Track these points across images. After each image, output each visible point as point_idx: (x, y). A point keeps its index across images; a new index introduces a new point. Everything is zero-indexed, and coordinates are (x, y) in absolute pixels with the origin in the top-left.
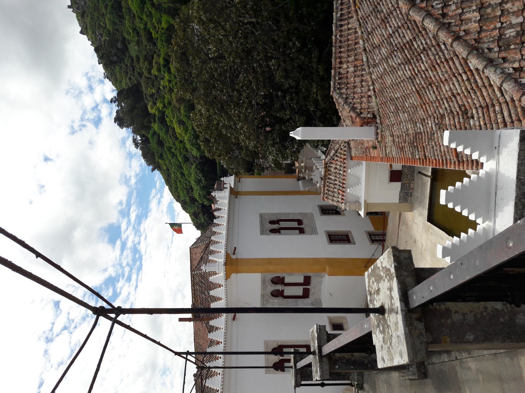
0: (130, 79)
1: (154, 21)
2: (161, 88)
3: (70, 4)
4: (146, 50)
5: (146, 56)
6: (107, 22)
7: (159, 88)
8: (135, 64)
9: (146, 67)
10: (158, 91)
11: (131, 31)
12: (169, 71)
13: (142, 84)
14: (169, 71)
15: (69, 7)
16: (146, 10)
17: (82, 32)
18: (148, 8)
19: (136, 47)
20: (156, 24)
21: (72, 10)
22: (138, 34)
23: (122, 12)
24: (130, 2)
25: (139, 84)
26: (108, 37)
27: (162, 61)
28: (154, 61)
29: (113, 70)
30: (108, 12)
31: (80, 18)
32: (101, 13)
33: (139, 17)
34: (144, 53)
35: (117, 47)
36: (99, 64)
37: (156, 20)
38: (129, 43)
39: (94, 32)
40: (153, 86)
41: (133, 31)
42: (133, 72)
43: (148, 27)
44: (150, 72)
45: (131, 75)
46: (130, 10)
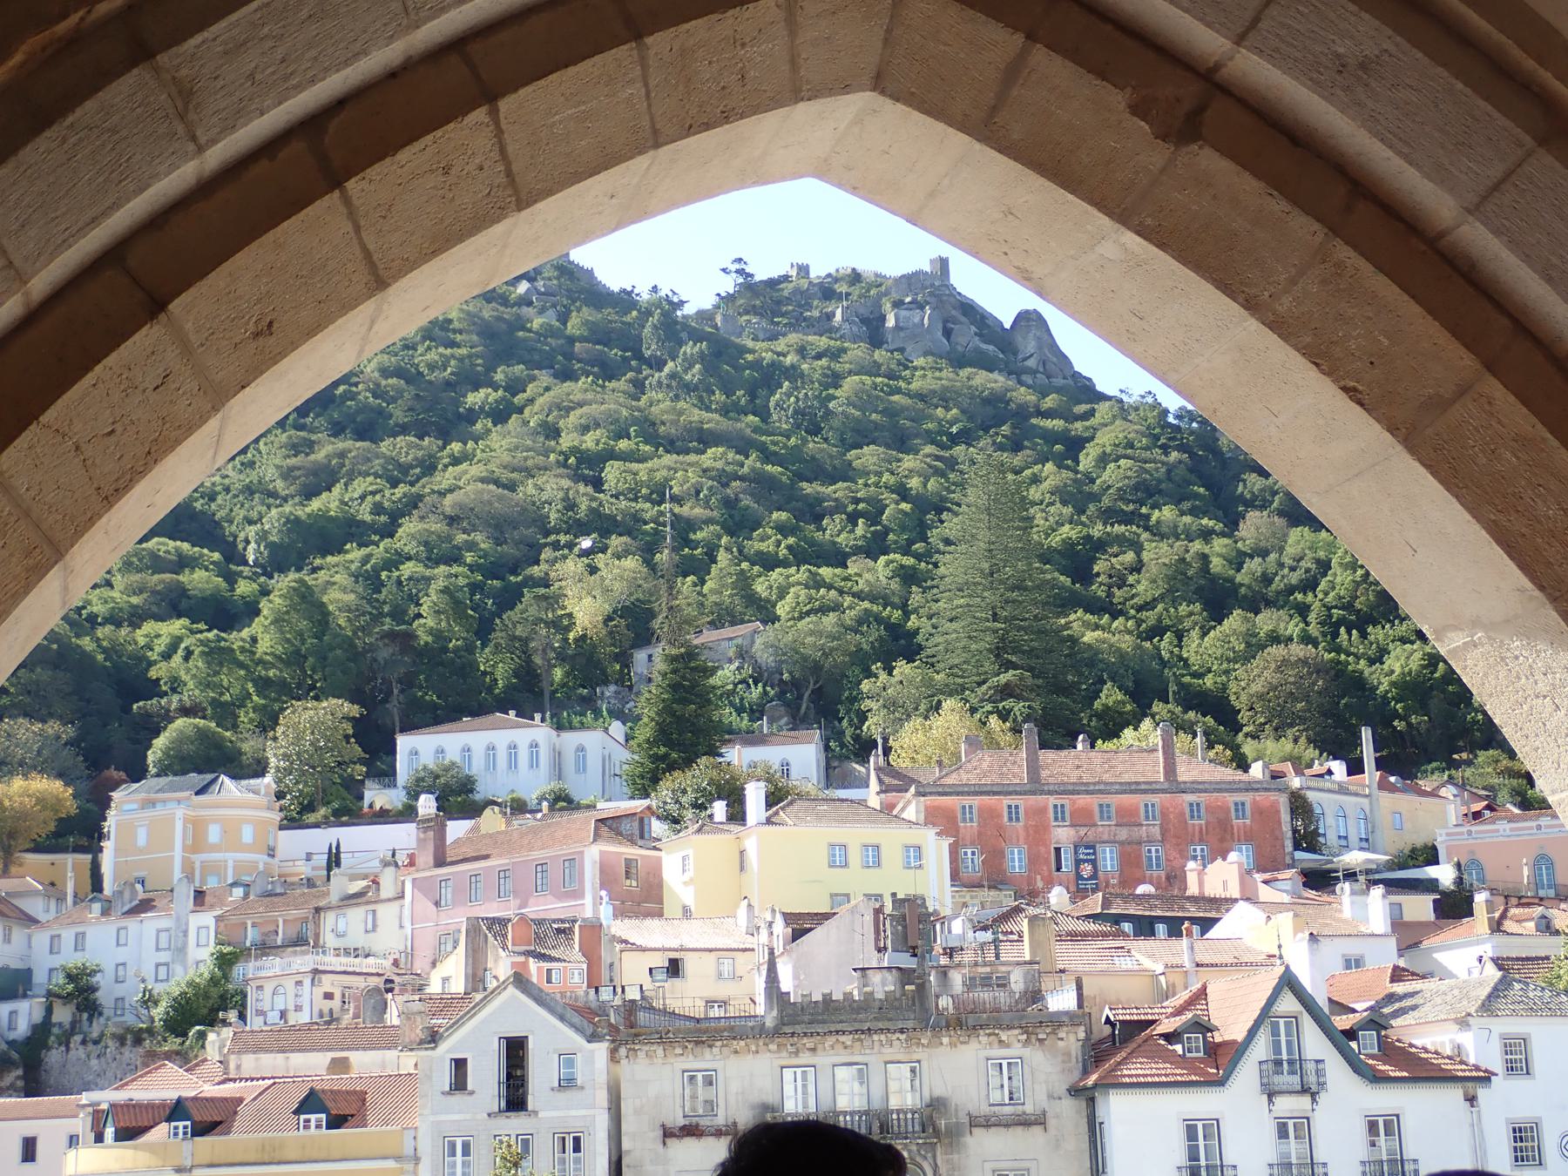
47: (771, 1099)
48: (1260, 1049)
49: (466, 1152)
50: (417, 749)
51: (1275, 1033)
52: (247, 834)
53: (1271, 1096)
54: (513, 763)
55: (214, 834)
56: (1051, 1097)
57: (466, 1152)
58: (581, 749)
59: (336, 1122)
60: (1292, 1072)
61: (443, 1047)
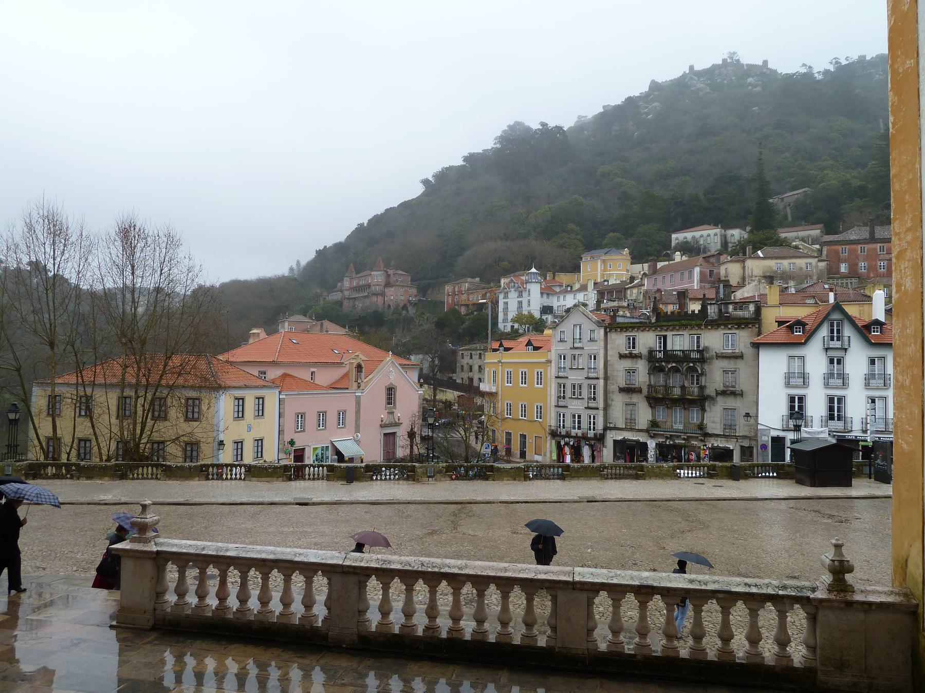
3: (696, 68)
17: (653, 82)
36: (604, 107)
47: (652, 346)
48: (824, 331)
50: (677, 237)
51: (832, 325)
53: (827, 349)
56: (745, 346)
59: (536, 349)
60: (838, 339)
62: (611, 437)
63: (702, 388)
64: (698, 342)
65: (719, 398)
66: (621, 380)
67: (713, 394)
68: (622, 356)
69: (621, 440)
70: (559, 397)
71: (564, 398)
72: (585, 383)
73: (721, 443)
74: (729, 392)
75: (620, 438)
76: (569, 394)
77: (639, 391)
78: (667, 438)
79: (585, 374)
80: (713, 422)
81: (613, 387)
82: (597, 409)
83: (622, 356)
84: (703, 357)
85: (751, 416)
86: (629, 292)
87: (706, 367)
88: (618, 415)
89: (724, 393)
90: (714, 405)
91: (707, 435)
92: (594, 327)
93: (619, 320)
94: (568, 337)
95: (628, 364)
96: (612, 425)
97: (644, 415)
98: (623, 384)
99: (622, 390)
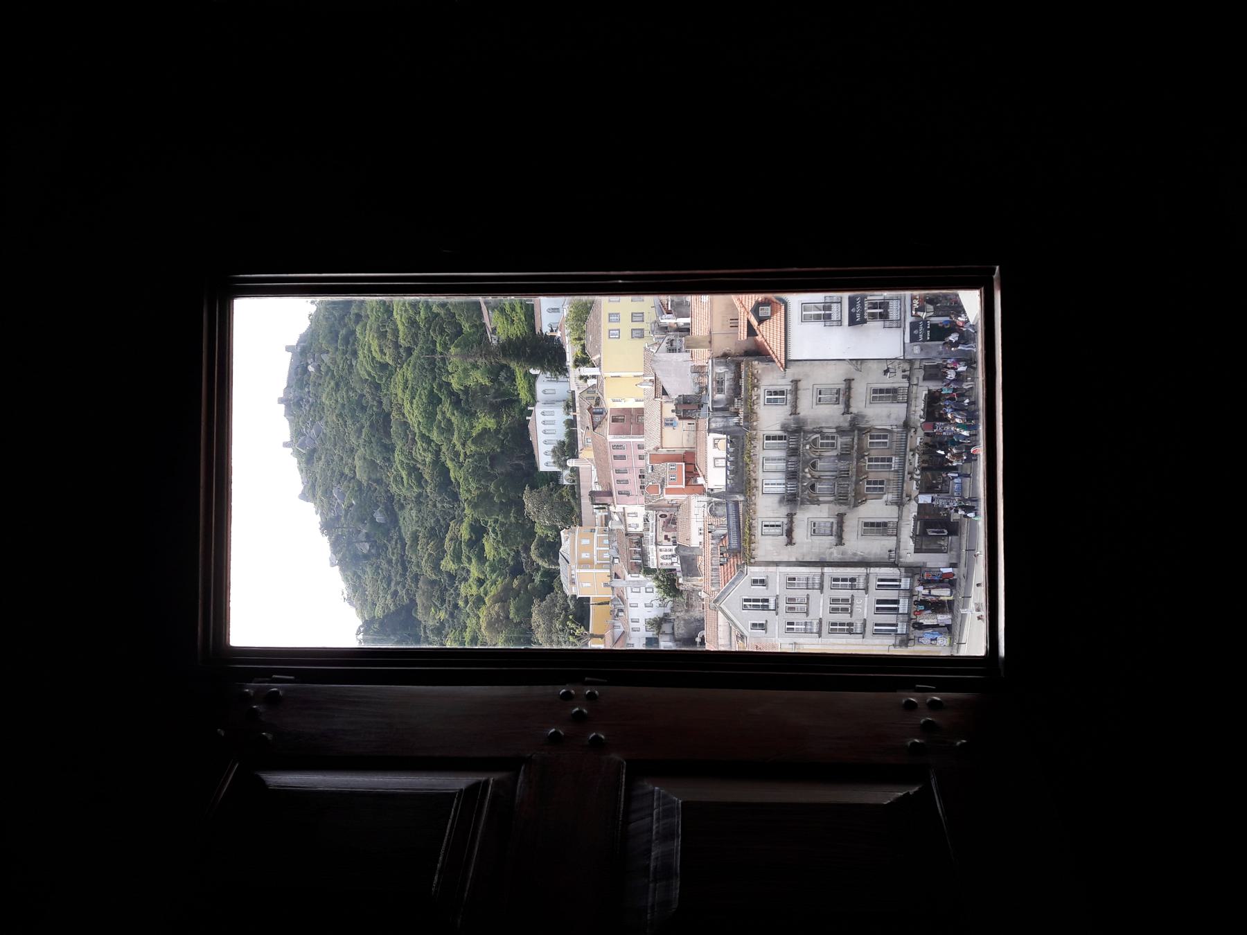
0: (395, 593)
1: (455, 439)
2: (461, 603)
3: (288, 439)
4: (434, 514)
5: (433, 528)
6: (358, 463)
7: (456, 606)
8: (408, 553)
9: (430, 555)
10: (452, 615)
11: (404, 474)
12: (482, 558)
13: (418, 601)
14: (482, 558)
15: (286, 445)
16: (439, 417)
17: (304, 496)
18: (444, 413)
19: (414, 513)
20: (459, 447)
21: (290, 450)
22: (420, 478)
23: (388, 435)
24: (407, 406)
25: (413, 602)
26: (356, 497)
27: (465, 533)
28: (448, 536)
29: (359, 577)
30: (361, 441)
31: (303, 465)
32: (347, 446)
33: (423, 436)
34: (431, 522)
35: (373, 519)
36: (333, 565)
37: (460, 437)
38: (402, 507)
39: (327, 492)
40: (443, 601)
41: (409, 475)
42: (403, 575)
43: (443, 459)
44: (436, 567)
45: (397, 583)
46: (405, 424)
47: (777, 498)
49: (792, 624)
50: (545, 462)
52: (585, 542)
54: (552, 423)
55: (585, 556)
56: (784, 377)
57: (789, 624)
58: (544, 392)
61: (746, 633)
62: (909, 554)
63: (841, 431)
64: (774, 438)
65: (854, 410)
66: (823, 546)
67: (849, 417)
68: (790, 542)
69: (915, 543)
70: (850, 632)
71: (850, 624)
72: (829, 593)
73: (919, 407)
74: (845, 394)
75: (911, 544)
76: (844, 617)
77: (841, 517)
78: (912, 478)
79: (814, 594)
80: (889, 416)
81: (836, 554)
82: (867, 575)
83: (790, 542)
84: (795, 431)
85: (887, 366)
86: (630, 530)
87: (809, 428)
88: (878, 546)
89: (848, 405)
90: (863, 417)
91: (907, 425)
92: (745, 581)
93: (734, 545)
94: (760, 616)
95: (800, 533)
96: (893, 554)
97: (877, 509)
98: (832, 539)
99: (840, 541)
